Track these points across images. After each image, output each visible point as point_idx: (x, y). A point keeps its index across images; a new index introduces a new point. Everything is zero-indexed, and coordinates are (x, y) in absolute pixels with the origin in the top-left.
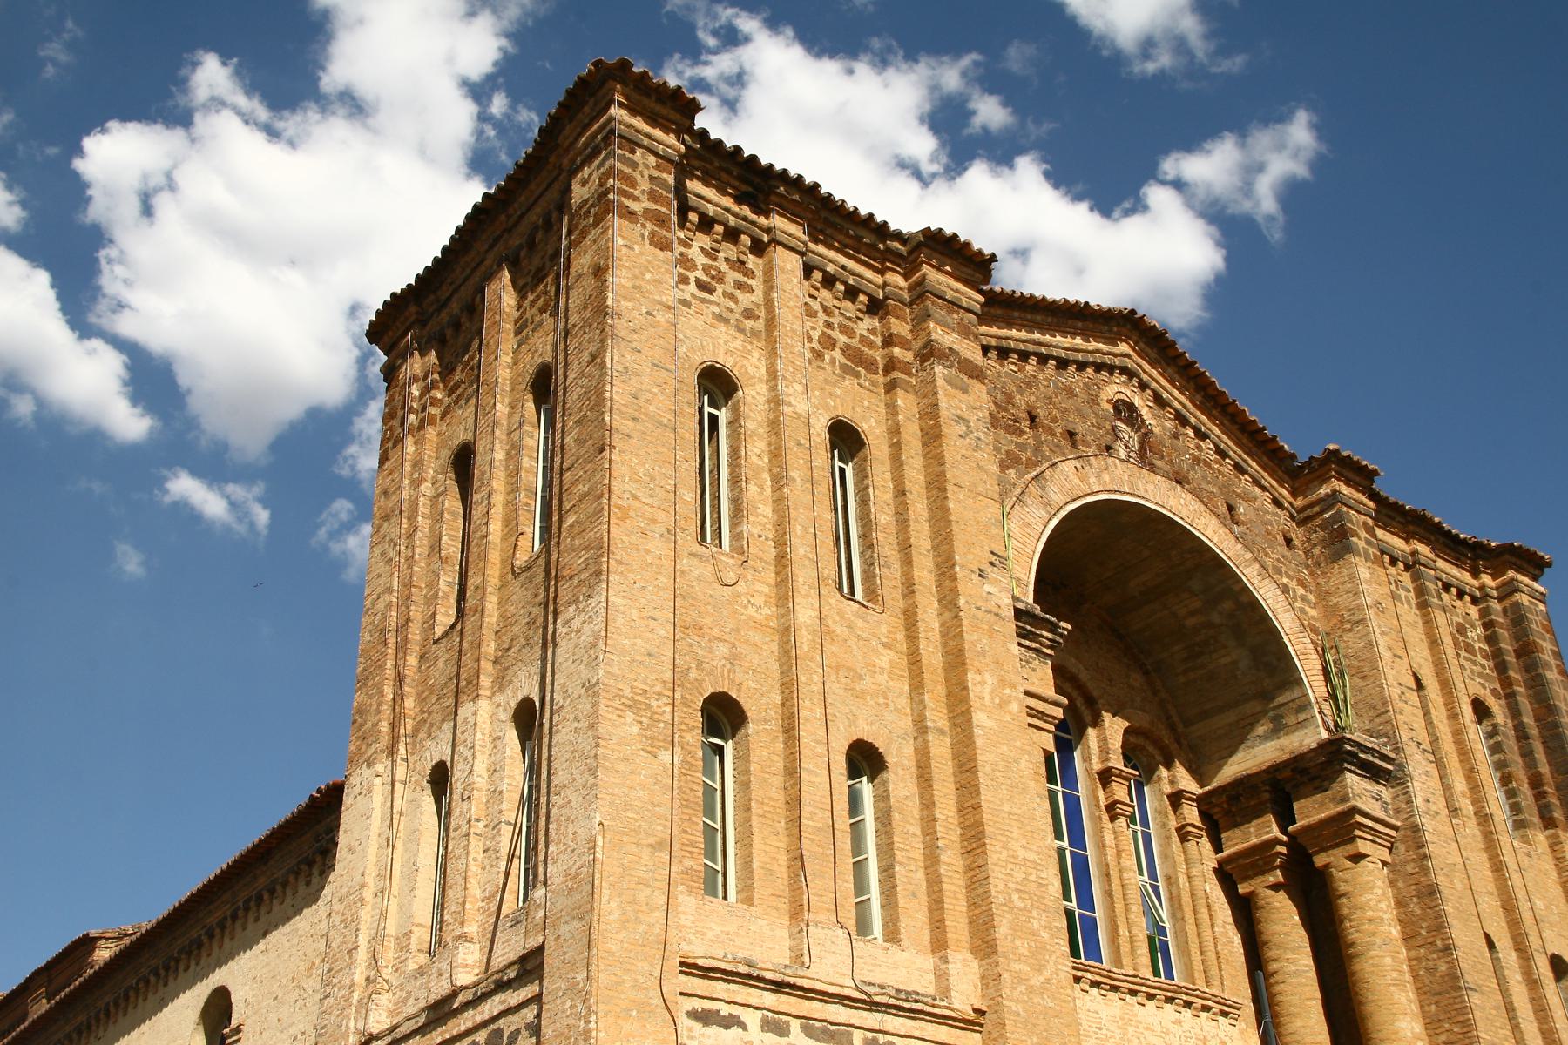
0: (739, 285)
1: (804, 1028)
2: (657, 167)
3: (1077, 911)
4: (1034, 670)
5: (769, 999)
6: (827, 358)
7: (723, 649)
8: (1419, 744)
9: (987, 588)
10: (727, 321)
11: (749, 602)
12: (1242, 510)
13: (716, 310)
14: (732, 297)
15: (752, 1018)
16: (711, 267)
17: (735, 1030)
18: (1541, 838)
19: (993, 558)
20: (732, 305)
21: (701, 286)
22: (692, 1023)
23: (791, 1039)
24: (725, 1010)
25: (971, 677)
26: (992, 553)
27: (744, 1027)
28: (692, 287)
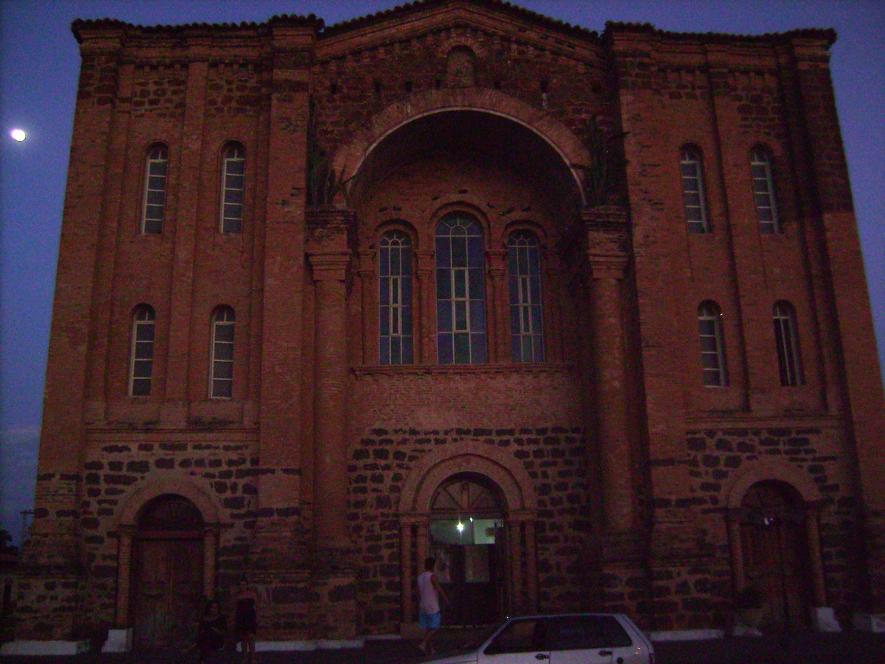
0: (175, 92)
1: (161, 445)
2: (107, 62)
3: (470, 333)
4: (333, 240)
5: (142, 436)
6: (226, 109)
7: (145, 282)
8: (650, 201)
9: (286, 210)
10: (164, 115)
11: (161, 255)
12: (555, 81)
13: (160, 111)
14: (169, 101)
15: (134, 447)
16: (158, 90)
17: (125, 453)
18: (793, 226)
19: (294, 191)
20: (168, 105)
21: (152, 102)
22: (105, 453)
23: (154, 452)
24: (120, 444)
25: (268, 261)
26: (294, 189)
27: (130, 450)
28: (147, 106)
